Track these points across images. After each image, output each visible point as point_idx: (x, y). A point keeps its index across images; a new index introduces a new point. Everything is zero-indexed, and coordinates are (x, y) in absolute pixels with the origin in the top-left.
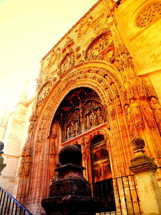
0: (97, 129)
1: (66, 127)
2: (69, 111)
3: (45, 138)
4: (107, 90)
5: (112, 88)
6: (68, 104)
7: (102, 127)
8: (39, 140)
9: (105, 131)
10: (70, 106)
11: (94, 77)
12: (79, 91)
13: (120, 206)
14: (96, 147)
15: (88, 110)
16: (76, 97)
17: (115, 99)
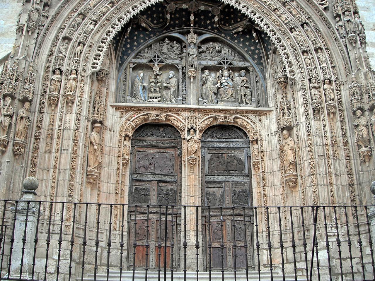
0: (236, 111)
1: (132, 66)
2: (148, 30)
3: (84, 70)
4: (305, 54)
5: (318, 58)
6: (155, 15)
7: (249, 113)
8: (64, 69)
9: (254, 123)
10: (155, 22)
11: (276, 9)
12: (205, 5)
13: (271, 264)
14: (215, 146)
15: (209, 58)
16: (188, 12)
17: (324, 84)
